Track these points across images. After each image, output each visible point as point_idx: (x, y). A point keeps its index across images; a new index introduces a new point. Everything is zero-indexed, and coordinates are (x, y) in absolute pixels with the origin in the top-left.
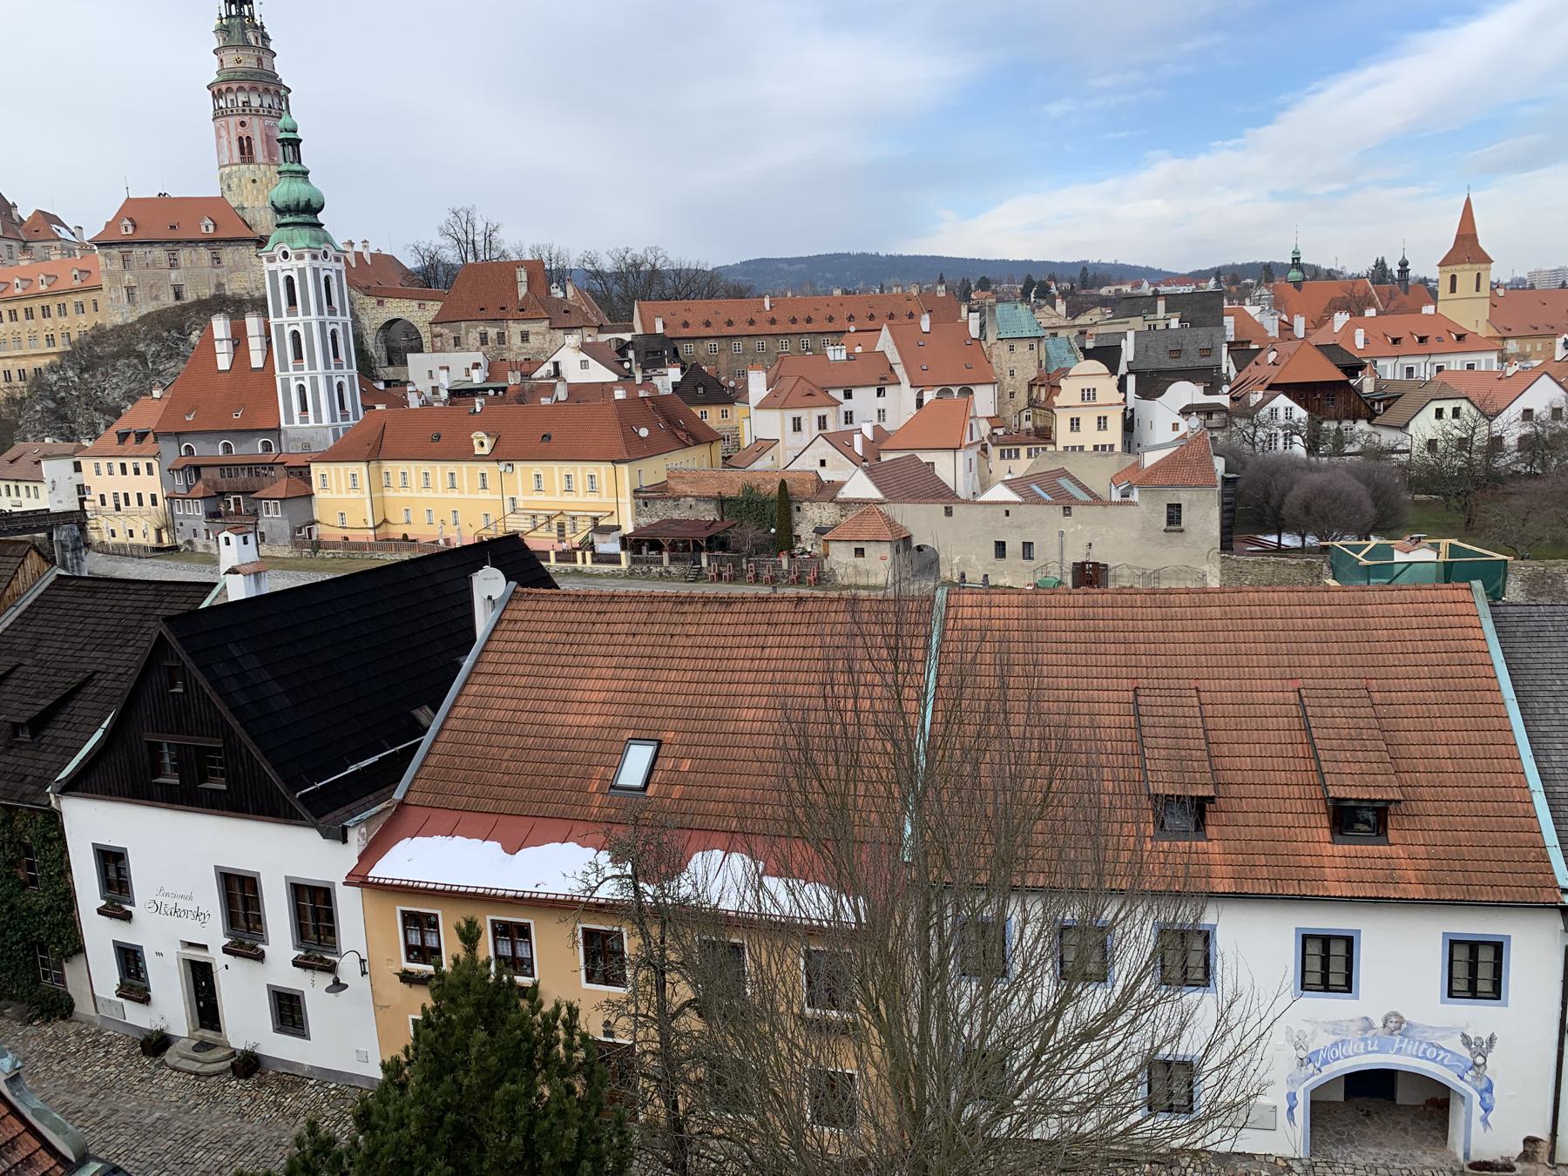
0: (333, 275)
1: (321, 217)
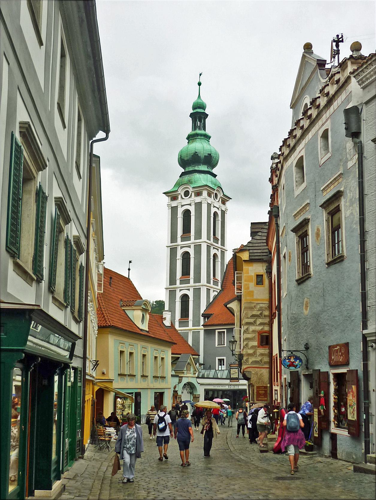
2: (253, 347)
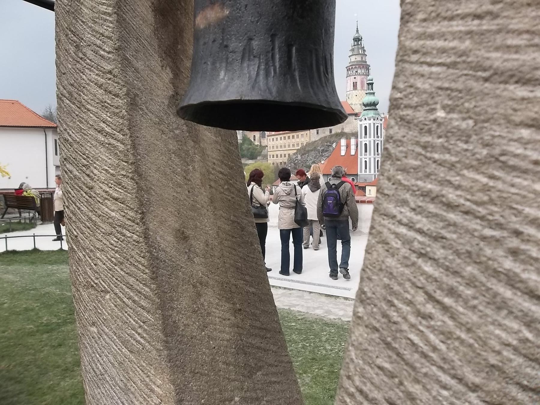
0: (379, 125)
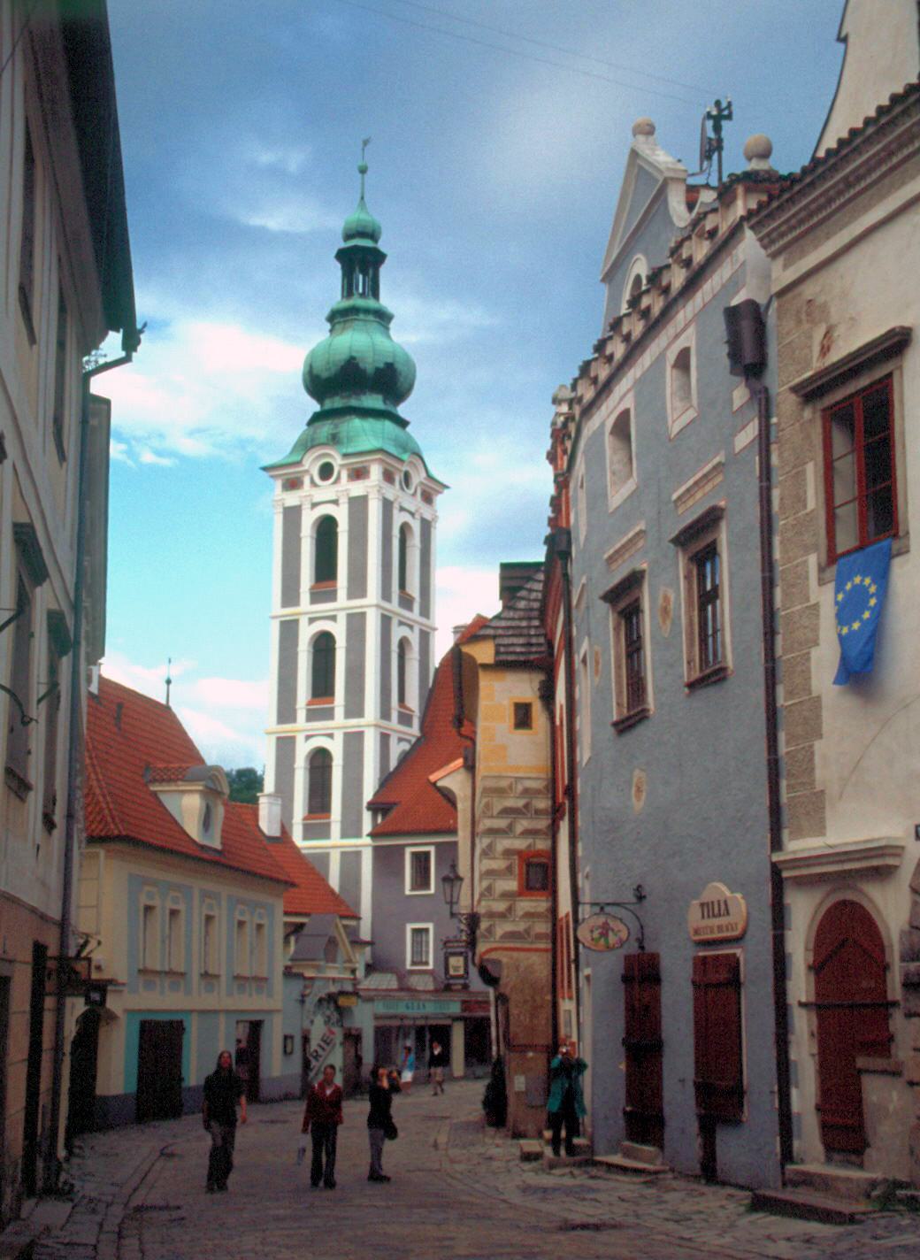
0: (416, 526)
1: (402, 410)
2: (506, 895)
